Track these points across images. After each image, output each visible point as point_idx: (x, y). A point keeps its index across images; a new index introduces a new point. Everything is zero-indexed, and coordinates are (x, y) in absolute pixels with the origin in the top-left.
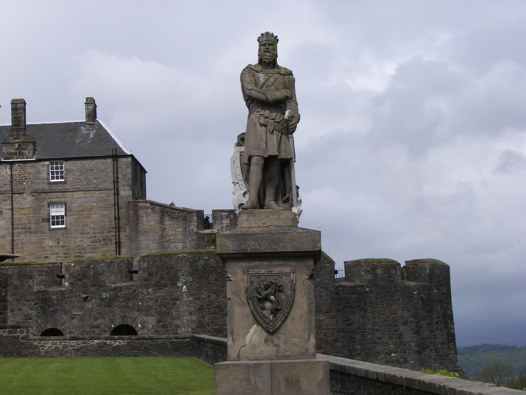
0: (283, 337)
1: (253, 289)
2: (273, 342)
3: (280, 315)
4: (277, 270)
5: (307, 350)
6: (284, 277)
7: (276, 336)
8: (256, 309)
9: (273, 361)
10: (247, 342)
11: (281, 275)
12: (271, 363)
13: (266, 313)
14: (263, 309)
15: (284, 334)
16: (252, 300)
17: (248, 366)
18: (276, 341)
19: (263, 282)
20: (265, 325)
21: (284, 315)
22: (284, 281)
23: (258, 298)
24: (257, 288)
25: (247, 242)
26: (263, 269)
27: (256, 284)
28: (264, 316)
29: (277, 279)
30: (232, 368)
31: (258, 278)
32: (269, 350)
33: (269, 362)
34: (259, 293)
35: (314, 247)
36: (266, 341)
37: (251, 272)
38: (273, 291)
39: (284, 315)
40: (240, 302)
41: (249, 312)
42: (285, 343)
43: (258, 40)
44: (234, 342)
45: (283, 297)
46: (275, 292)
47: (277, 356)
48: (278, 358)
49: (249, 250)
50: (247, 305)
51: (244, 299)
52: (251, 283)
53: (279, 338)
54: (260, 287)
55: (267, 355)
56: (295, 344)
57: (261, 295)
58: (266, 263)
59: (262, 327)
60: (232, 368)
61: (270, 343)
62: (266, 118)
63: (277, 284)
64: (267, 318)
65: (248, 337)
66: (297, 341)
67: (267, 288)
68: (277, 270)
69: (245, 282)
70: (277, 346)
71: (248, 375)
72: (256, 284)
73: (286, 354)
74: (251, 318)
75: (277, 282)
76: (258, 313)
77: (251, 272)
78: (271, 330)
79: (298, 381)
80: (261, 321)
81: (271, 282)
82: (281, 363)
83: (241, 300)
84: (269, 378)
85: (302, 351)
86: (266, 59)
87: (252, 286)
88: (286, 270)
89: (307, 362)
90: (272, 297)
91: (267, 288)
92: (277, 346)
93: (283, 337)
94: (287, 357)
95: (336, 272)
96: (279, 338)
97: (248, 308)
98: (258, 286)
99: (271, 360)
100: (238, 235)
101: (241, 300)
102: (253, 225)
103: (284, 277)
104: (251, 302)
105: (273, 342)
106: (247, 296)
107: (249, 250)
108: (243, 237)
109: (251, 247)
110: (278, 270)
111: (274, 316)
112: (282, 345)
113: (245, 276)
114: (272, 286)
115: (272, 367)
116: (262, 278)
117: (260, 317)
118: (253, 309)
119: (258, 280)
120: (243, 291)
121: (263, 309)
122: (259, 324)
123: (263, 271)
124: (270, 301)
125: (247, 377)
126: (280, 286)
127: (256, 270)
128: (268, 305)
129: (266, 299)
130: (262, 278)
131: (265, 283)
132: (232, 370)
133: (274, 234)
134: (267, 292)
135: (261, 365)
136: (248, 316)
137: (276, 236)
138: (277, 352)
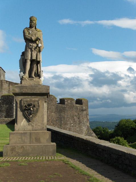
0: (35, 123)
2: (31, 125)
5: (43, 128)
9: (31, 132)
10: (22, 125)
11: (34, 101)
12: (30, 133)
17: (22, 133)
18: (32, 124)
22: (36, 103)
25: (23, 89)
32: (30, 127)
33: (30, 132)
35: (47, 91)
42: (35, 125)
43: (30, 19)
47: (32, 130)
48: (33, 130)
55: (29, 129)
56: (39, 126)
58: (30, 97)
60: (16, 134)
61: (30, 125)
66: (40, 124)
68: (33, 99)
70: (33, 126)
71: (22, 136)
72: (26, 104)
73: (36, 129)
79: (39, 139)
82: (33, 132)
84: (29, 138)
85: (42, 128)
88: (37, 99)
89: (43, 132)
93: (35, 123)
94: (36, 130)
95: (57, 101)
99: (30, 131)
100: (20, 86)
102: (26, 83)
105: (31, 125)
108: (22, 87)
109: (25, 91)
112: (34, 126)
115: (30, 133)
123: (28, 100)
125: (21, 137)
132: (16, 135)
133: (33, 87)
135: (26, 133)
137: (34, 87)
138: (33, 128)
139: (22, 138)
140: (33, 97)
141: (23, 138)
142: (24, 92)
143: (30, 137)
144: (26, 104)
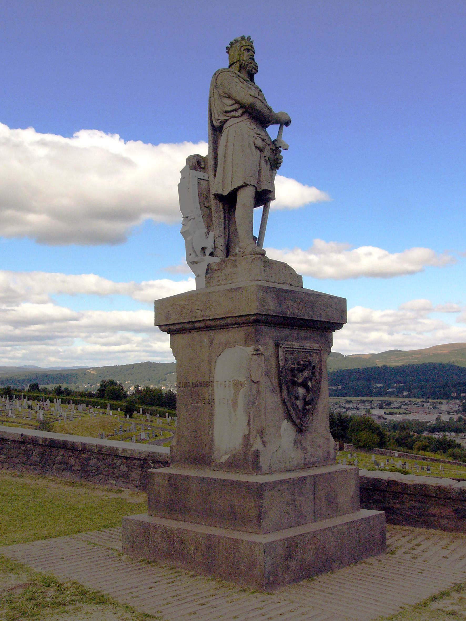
2: (301, 443)
4: (308, 345)
5: (329, 453)
11: (310, 352)
14: (297, 398)
20: (298, 421)
22: (315, 359)
30: (278, 486)
36: (295, 443)
37: (286, 344)
40: (271, 387)
42: (311, 446)
44: (265, 447)
49: (289, 313)
52: (286, 360)
56: (319, 446)
58: (294, 333)
59: (293, 422)
61: (299, 445)
62: (263, 140)
68: (308, 345)
70: (304, 449)
73: (313, 460)
80: (294, 416)
86: (253, 67)
92: (304, 449)
104: (284, 387)
107: (289, 313)
112: (309, 448)
118: (287, 399)
121: (297, 398)
123: (296, 345)
127: (290, 343)
138: (305, 458)
139: (295, 500)
140: (303, 333)
141: (297, 498)
142: (289, 314)
143: (314, 494)
144: (290, 362)
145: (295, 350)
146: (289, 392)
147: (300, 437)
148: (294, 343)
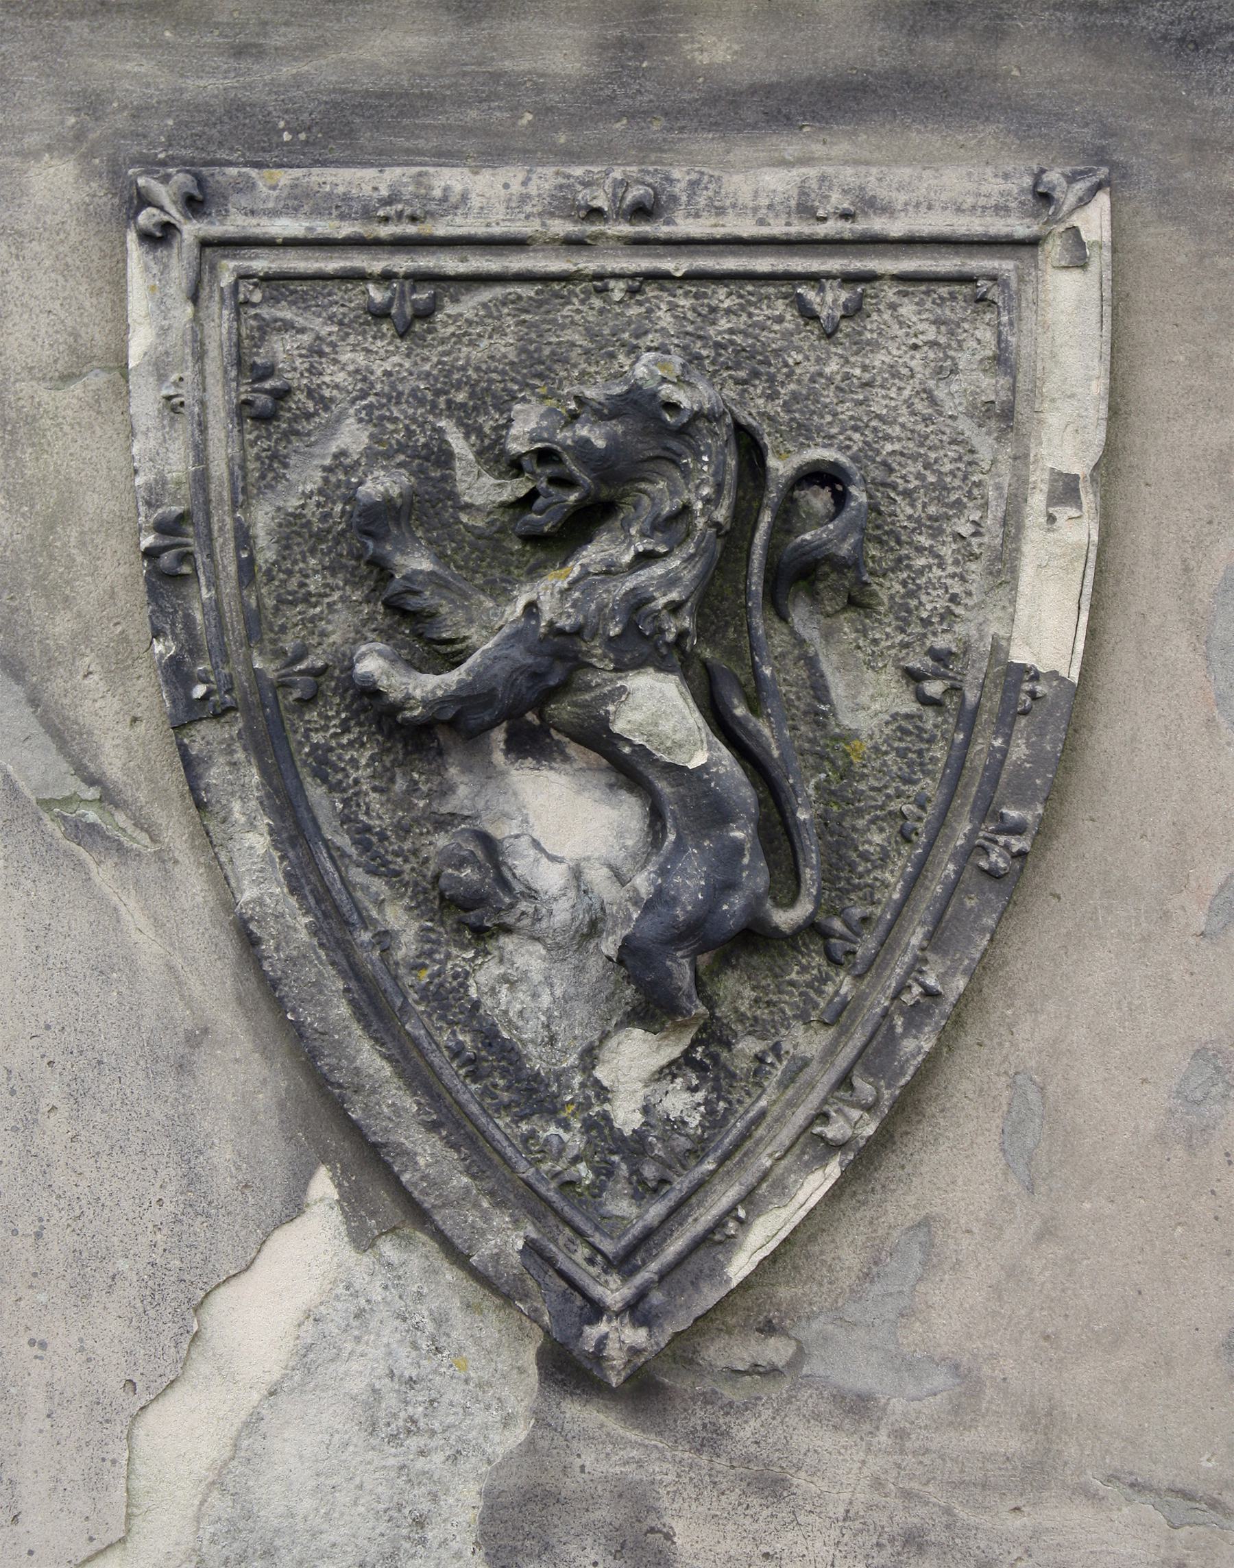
1: (292, 529)
3: (806, 1041)
4: (752, 188)
6: (903, 323)
7: (709, 1441)
8: (335, 919)
13: (528, 988)
15: (857, 1407)
16: (270, 745)
19: (484, 400)
21: (877, 1053)
22: (890, 383)
23: (367, 698)
24: (378, 520)
26: (495, 152)
27: (352, 437)
28: (495, 1052)
29: (751, 363)
31: (412, 324)
34: (415, 629)
37: (271, 205)
38: (672, 577)
39: (877, 1053)
41: (213, 983)
45: (868, 701)
46: (715, 598)
50: (175, 829)
51: (120, 717)
52: (268, 410)
53: (770, 1485)
54: (427, 507)
57: (443, 654)
63: (749, 446)
64: (536, 1097)
65: (183, 1436)
67: (570, 504)
68: (752, 188)
69: (145, 401)
72: (352, 437)
74: (242, 1081)
75: (755, 408)
76: (376, 1007)
77: (271, 205)
78: (620, 1339)
80: (426, 1156)
81: (639, 406)
83: (62, 734)
87: (275, 462)
88: (942, 185)
90: (655, 707)
91: (570, 504)
96: (770, 1485)
97: (194, 887)
98: (381, 484)
101: (62, 734)
103: (903, 323)
106: (177, 673)
110: (778, 182)
111: (704, 1062)
113: (151, 307)
114: (661, 495)
116: (479, 336)
117: (415, 1072)
118: (291, 925)
119: (384, 357)
120: (108, 574)
121: (477, 907)
122: (385, 1198)
123: (488, 195)
124: (628, 768)
126: (825, 477)
128: (563, 829)
129: (541, 708)
130: (479, 336)
131: (525, 426)
134: (549, 594)
136: (198, 1037)
145: (450, 263)
146: (294, 829)
147: (605, 1447)
148: (450, 179)
